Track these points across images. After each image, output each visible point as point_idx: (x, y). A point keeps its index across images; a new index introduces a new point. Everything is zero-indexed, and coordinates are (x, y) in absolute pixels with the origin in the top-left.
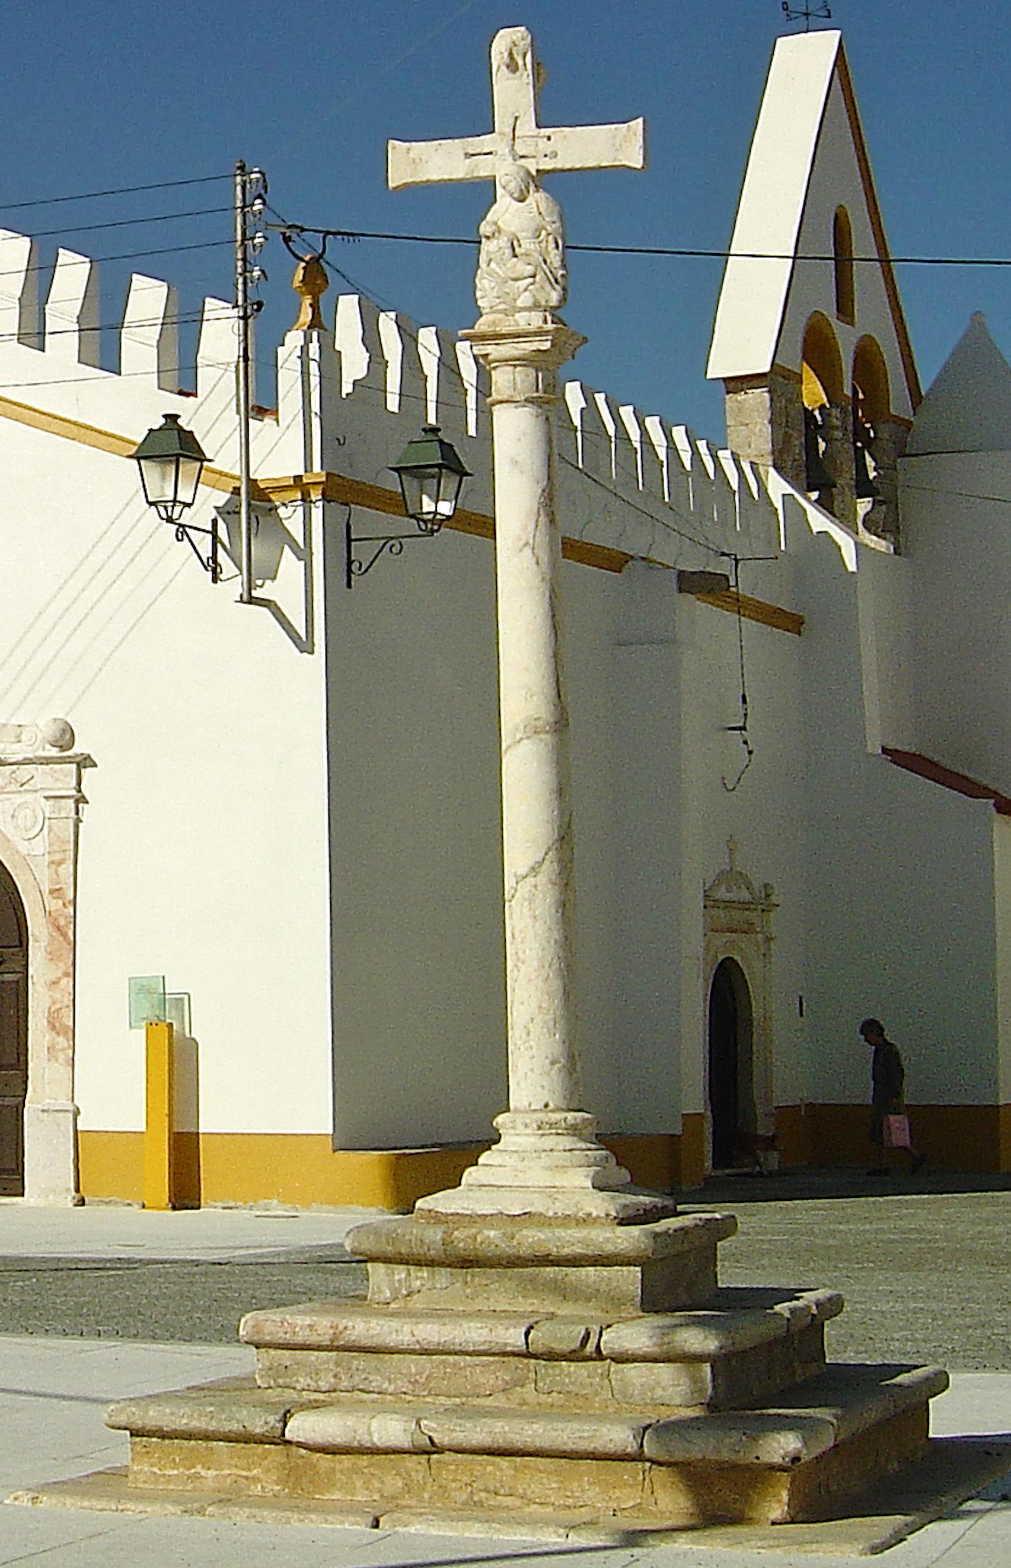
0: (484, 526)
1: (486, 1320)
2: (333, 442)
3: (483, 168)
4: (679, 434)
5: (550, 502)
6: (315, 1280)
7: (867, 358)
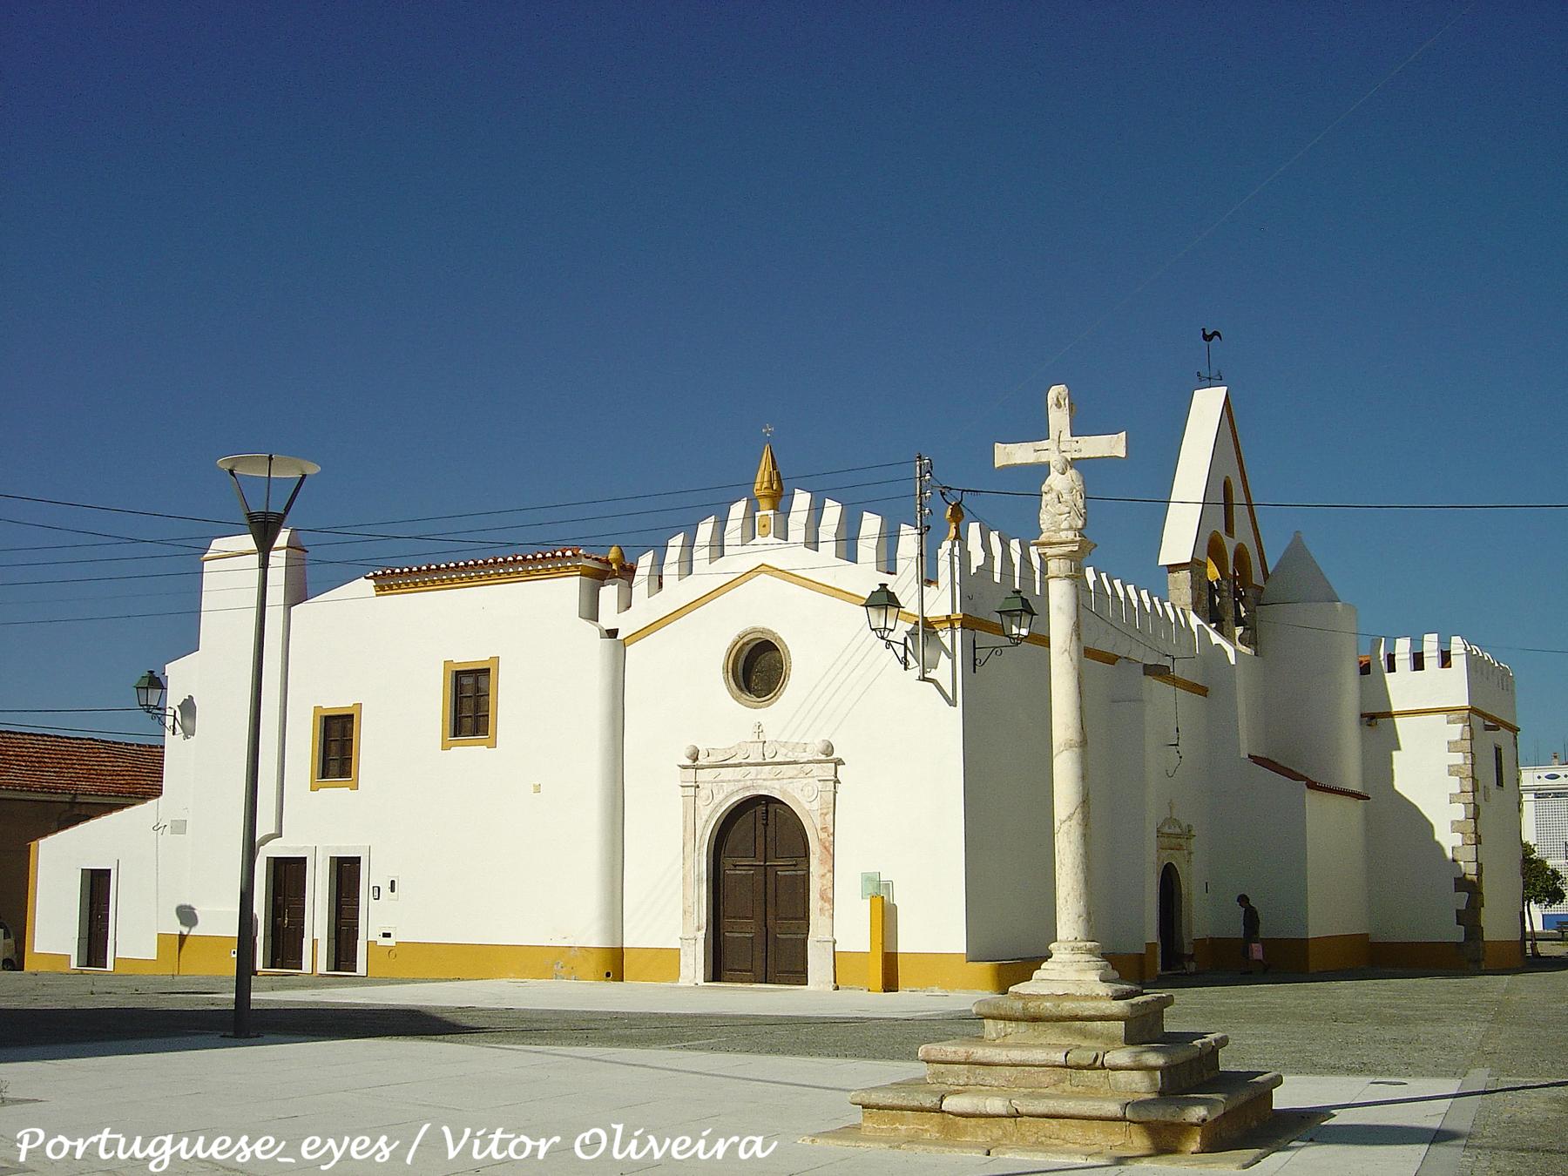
0: (1045, 641)
1: (1045, 1048)
2: (966, 598)
3: (1043, 457)
4: (1144, 593)
5: (1078, 629)
6: (957, 1028)
7: (1241, 555)
